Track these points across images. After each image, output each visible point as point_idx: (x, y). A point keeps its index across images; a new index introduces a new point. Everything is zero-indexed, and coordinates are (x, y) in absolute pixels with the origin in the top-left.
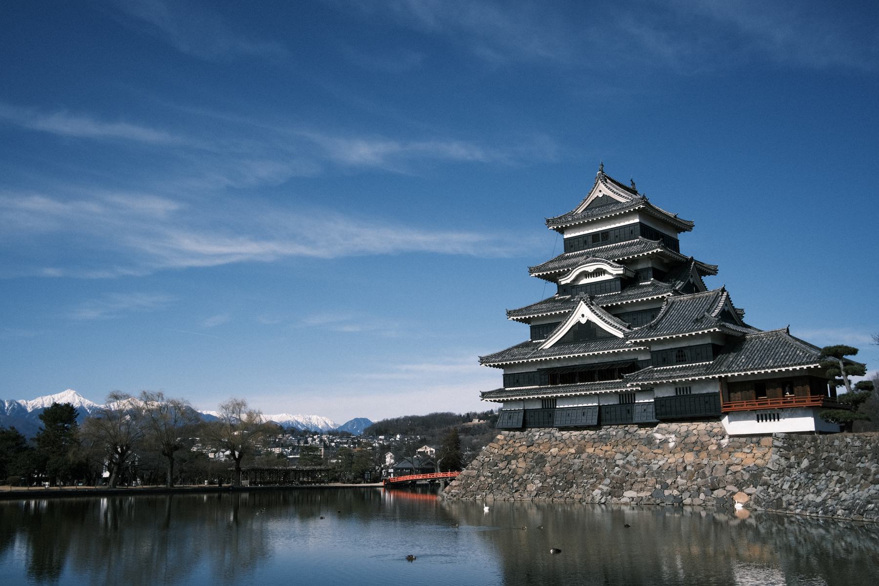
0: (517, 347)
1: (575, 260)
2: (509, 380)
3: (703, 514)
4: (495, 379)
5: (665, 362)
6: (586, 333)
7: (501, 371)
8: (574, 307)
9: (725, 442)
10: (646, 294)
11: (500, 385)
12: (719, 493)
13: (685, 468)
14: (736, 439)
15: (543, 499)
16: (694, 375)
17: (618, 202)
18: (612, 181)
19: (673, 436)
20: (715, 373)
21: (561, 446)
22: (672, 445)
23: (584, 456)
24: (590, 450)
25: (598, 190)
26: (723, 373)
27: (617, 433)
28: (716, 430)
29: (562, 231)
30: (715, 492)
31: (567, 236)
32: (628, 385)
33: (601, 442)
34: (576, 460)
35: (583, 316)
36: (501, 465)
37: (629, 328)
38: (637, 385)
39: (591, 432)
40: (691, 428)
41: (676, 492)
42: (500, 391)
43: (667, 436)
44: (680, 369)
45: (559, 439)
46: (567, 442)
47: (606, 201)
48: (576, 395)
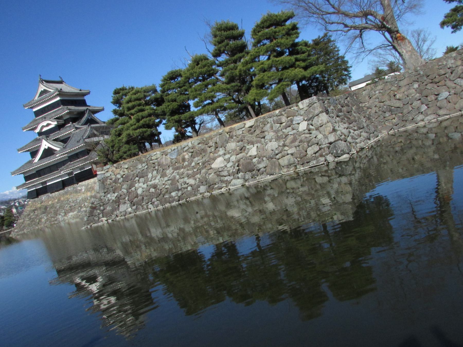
0: (26, 164)
2: (27, 178)
4: (21, 179)
6: (49, 152)
11: (23, 181)
17: (50, 92)
22: (83, 190)
24: (62, 199)
29: (32, 108)
41: (84, 209)
47: (44, 92)
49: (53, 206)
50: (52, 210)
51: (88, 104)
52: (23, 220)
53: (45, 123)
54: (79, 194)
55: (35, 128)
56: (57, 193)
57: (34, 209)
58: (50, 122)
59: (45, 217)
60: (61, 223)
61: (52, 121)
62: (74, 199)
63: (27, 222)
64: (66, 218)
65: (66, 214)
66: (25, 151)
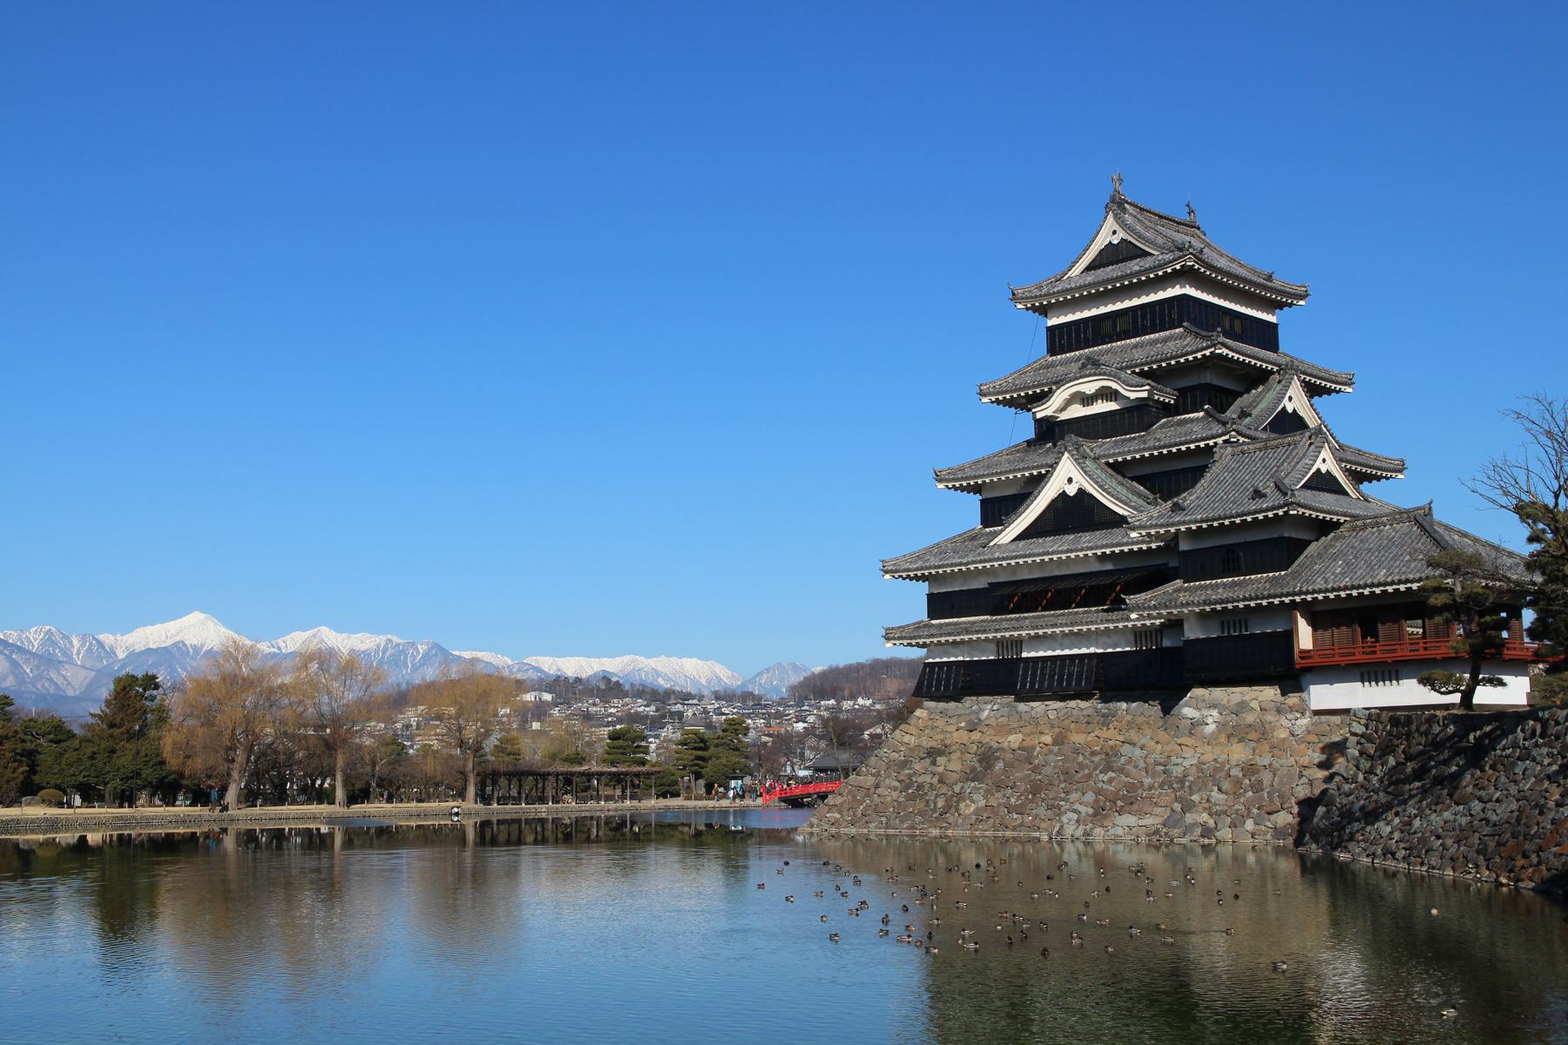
0: (952, 540)
2: (939, 605)
4: (912, 602)
6: (1074, 514)
7: (924, 588)
8: (1053, 466)
11: (920, 612)
15: (987, 832)
17: (1148, 254)
19: (1215, 713)
22: (1211, 728)
24: (1077, 738)
29: (1044, 311)
32: (1133, 616)
34: (1052, 757)
35: (1070, 480)
36: (917, 766)
38: (1160, 616)
39: (1083, 704)
40: (1247, 698)
41: (1204, 817)
42: (919, 626)
43: (1205, 712)
49: (1025, 755)
55: (1042, 397)
57: (934, 744)
58: (1114, 386)
60: (1069, 847)
64: (1098, 831)
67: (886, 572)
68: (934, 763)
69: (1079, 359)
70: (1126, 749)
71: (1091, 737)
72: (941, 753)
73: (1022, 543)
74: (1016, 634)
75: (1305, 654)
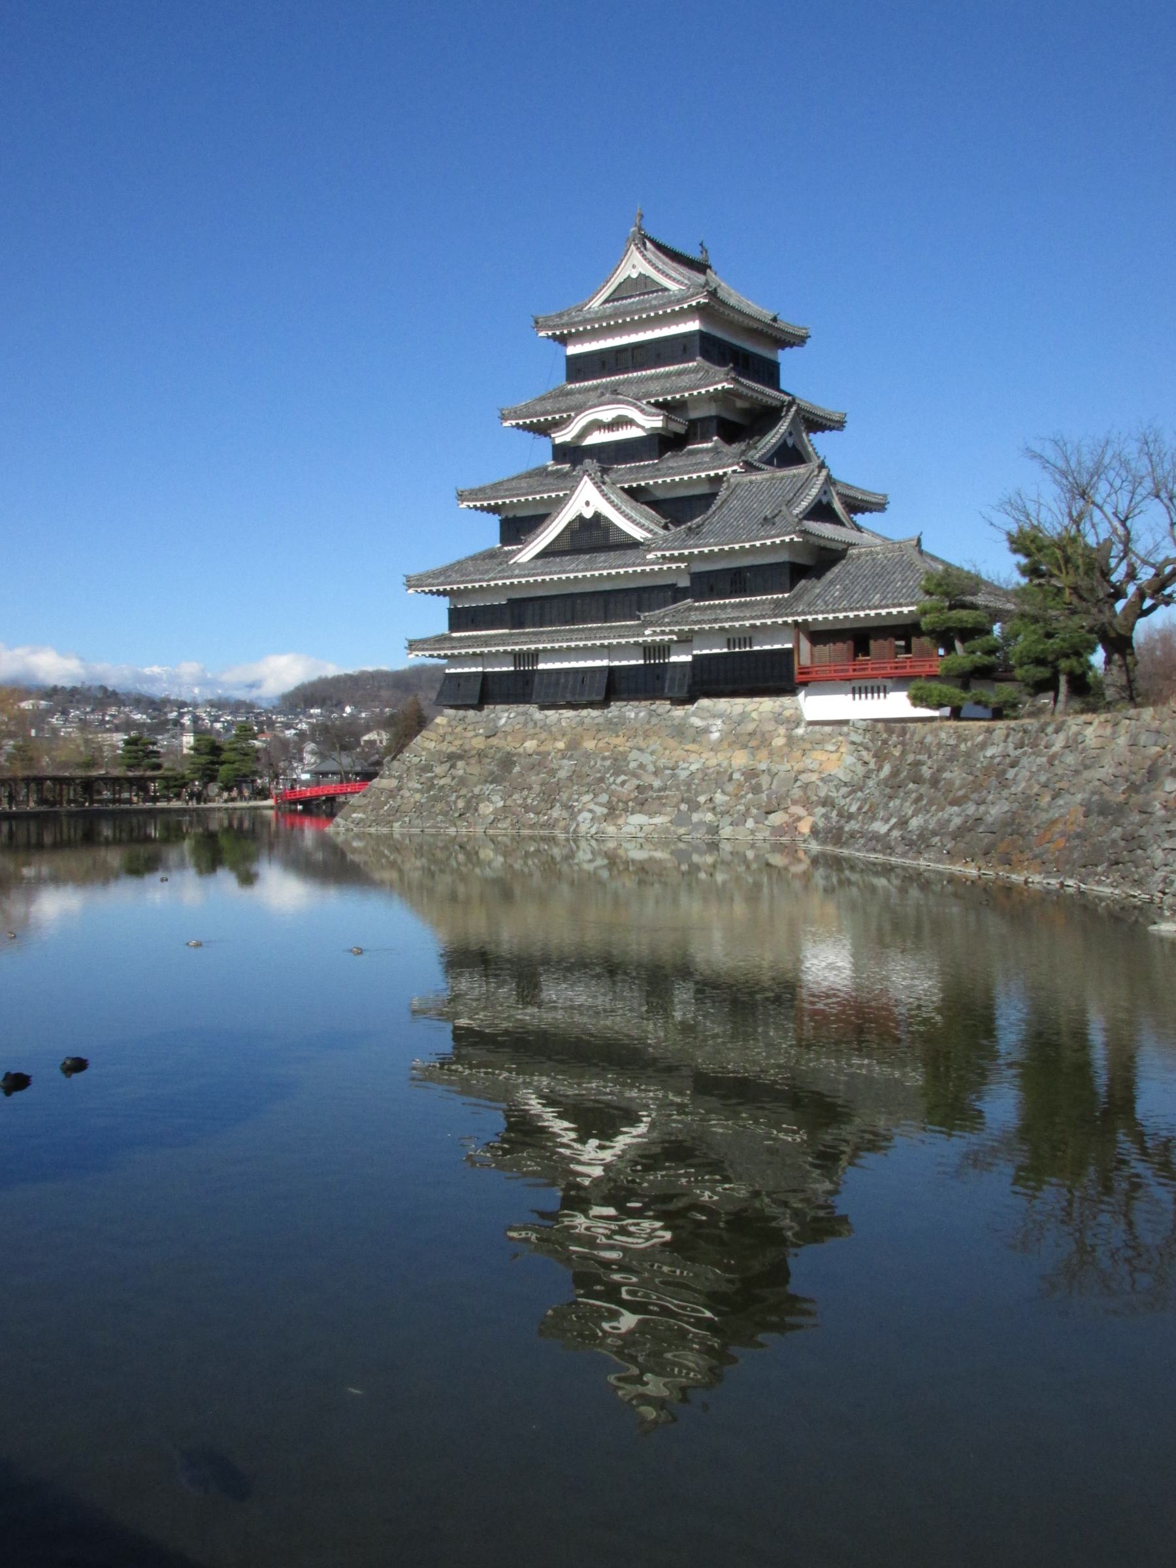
0: (473, 558)
1: (580, 398)
2: (459, 618)
3: (750, 854)
4: (434, 617)
5: (713, 593)
6: (590, 536)
7: (444, 603)
8: (573, 489)
9: (800, 731)
10: (698, 467)
11: (441, 626)
12: (777, 819)
13: (730, 779)
14: (817, 728)
16: (753, 618)
17: (666, 289)
18: (660, 247)
19: (719, 722)
20: (787, 615)
21: (543, 736)
22: (715, 736)
23: (576, 754)
24: (589, 745)
25: (629, 265)
26: (799, 614)
27: (637, 714)
28: (787, 713)
29: (563, 340)
30: (771, 816)
31: (573, 350)
32: (647, 632)
33: (609, 729)
34: (565, 762)
35: (587, 504)
36: (439, 770)
37: (666, 527)
38: (672, 632)
40: (749, 709)
41: (709, 817)
42: (440, 640)
44: (733, 606)
45: (539, 724)
46: (554, 729)
47: (642, 284)
48: (569, 648)
49: (539, 762)
50: (534, 779)
51: (783, 386)
52: (394, 783)
53: (607, 414)
54: (690, 747)
55: (558, 425)
56: (568, 713)
59: (496, 798)
60: (583, 844)
61: (642, 411)
62: (662, 762)
63: (413, 793)
64: (611, 830)
65: (612, 813)
66: (482, 508)
67: (410, 587)
68: (453, 766)
69: (596, 388)
70: (634, 754)
71: (601, 744)
72: (460, 757)
73: (540, 562)
74: (533, 647)
75: (804, 671)
